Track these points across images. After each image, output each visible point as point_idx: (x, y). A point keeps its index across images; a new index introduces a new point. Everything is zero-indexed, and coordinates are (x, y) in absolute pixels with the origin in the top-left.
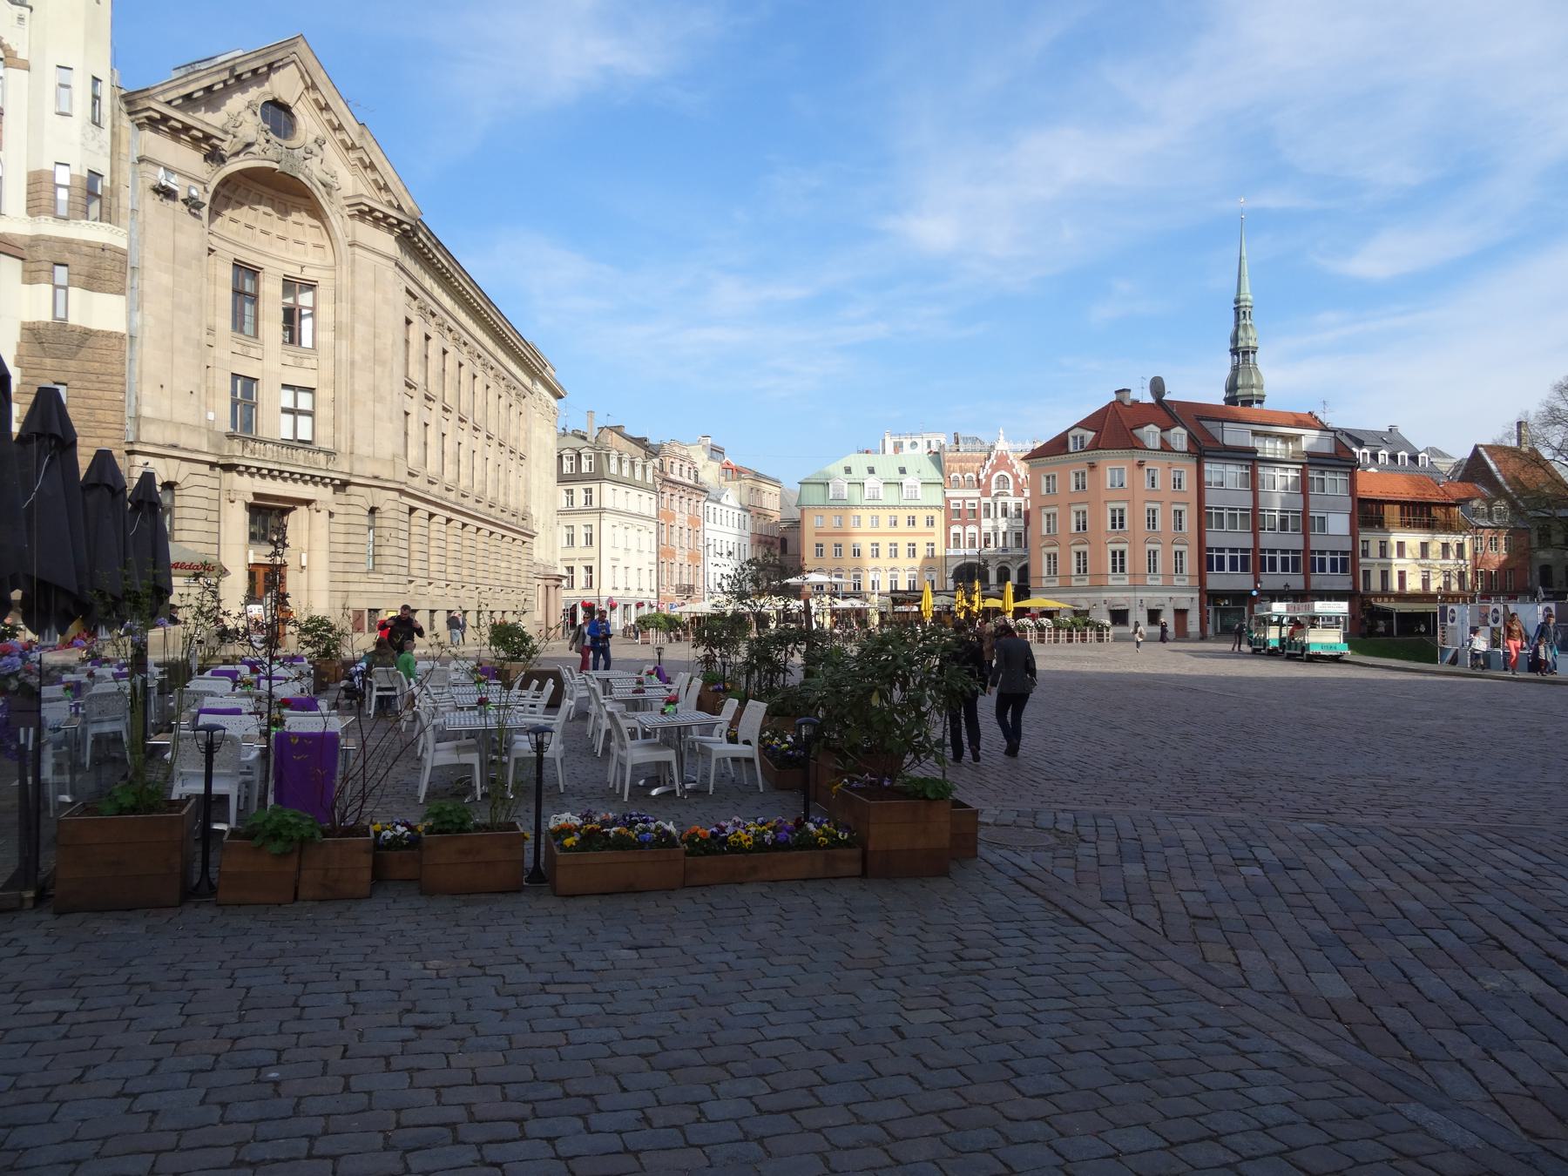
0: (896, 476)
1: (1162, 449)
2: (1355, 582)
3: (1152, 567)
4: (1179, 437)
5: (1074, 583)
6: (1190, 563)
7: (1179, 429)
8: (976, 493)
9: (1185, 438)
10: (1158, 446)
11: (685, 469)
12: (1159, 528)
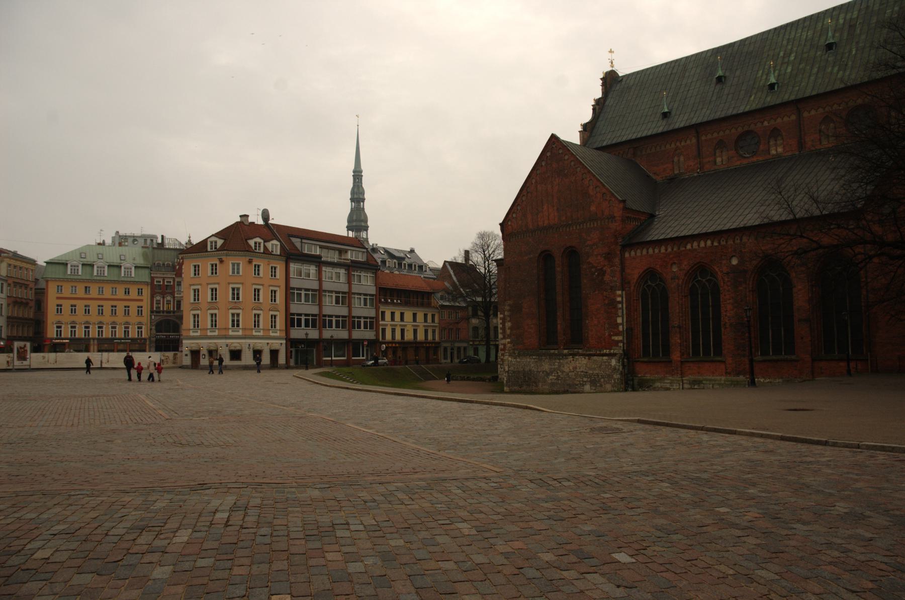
0: (116, 260)
1: (264, 253)
2: (377, 335)
3: (257, 324)
4: (274, 246)
5: (209, 334)
6: (280, 323)
7: (275, 242)
8: (172, 275)
9: (279, 247)
10: (262, 251)
12: (261, 300)
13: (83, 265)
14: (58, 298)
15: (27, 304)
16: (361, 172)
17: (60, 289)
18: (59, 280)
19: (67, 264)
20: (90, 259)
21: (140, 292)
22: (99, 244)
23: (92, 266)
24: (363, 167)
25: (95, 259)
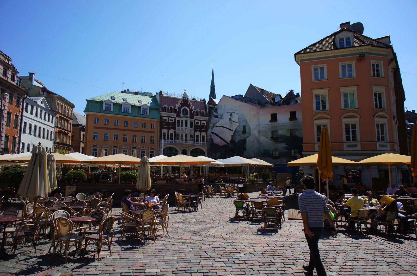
11: (10, 72)
14: (95, 127)
15: (68, 133)
16: (215, 86)
22: (122, 92)
25: (123, 101)
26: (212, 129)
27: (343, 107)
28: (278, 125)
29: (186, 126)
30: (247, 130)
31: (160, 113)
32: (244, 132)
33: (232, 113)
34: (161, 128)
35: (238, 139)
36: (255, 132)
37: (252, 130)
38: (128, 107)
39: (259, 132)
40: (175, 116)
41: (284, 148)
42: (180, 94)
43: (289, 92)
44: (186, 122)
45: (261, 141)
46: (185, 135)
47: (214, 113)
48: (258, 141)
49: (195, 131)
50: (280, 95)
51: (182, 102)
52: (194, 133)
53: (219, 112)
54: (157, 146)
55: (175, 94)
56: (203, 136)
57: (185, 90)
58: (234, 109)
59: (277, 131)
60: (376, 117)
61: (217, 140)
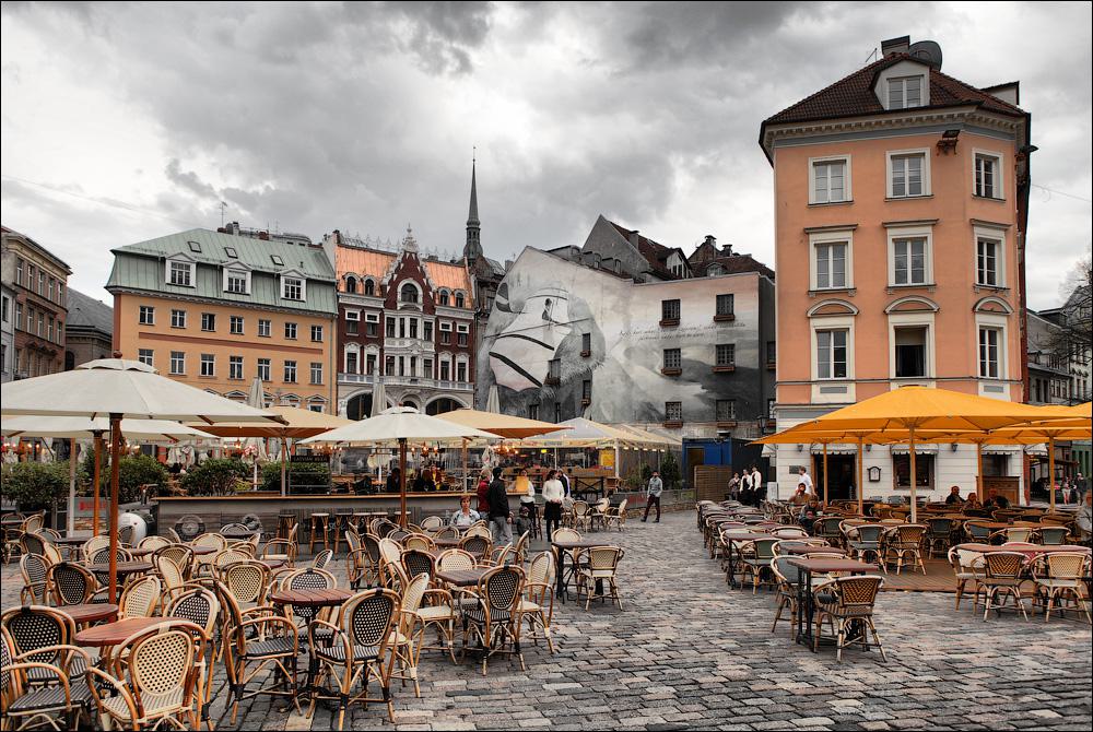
0: (268, 267)
13: (199, 265)
14: (142, 335)
15: (54, 354)
17: (145, 317)
18: (147, 294)
19: (163, 260)
20: (212, 255)
21: (315, 334)
22: (220, 230)
23: (218, 269)
24: (481, 218)
26: (492, 343)
27: (892, 283)
28: (682, 333)
29: (414, 335)
30: (594, 348)
31: (338, 297)
32: (586, 355)
33: (551, 299)
34: (342, 341)
35: (568, 371)
36: (617, 353)
37: (607, 346)
38: (242, 277)
39: (628, 352)
40: (382, 306)
41: (699, 396)
42: (394, 243)
43: (704, 241)
44: (414, 322)
45: (633, 376)
46: (409, 360)
47: (498, 298)
48: (626, 378)
49: (439, 348)
50: (680, 250)
51: (399, 265)
52: (437, 356)
53: (514, 295)
54: (331, 390)
55: (378, 241)
56: (462, 365)
57: (409, 231)
58: (556, 285)
59: (679, 350)
60: (981, 310)
61: (506, 376)
